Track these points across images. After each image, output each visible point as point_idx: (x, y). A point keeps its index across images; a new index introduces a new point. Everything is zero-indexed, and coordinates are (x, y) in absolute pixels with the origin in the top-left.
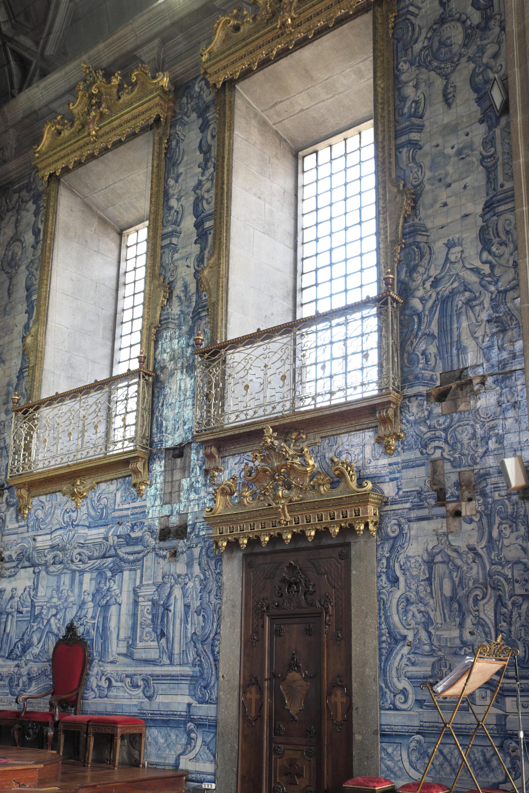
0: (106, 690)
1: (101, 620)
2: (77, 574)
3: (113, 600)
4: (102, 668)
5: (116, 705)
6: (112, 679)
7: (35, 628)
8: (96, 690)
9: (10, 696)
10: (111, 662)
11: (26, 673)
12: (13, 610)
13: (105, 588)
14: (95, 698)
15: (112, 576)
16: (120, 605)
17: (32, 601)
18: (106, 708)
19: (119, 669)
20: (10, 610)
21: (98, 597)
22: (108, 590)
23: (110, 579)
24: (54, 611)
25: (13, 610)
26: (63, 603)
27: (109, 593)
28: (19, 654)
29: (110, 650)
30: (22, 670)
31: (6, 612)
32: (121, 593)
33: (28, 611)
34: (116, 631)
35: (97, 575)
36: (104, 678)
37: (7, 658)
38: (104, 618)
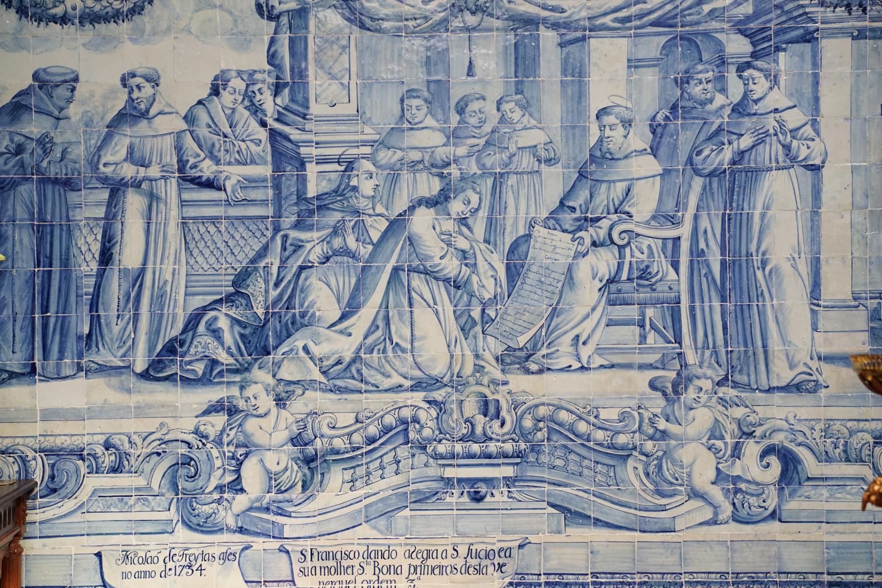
0: (773, 491)
1: (711, 224)
2: (548, 38)
3: (772, 150)
4: (739, 412)
5: (829, 546)
6: (803, 453)
7: (315, 253)
8: (716, 493)
9: (182, 534)
10: (786, 389)
11: (282, 436)
12: (154, 171)
13: (720, 100)
14: (714, 522)
15: (755, 55)
16: (815, 169)
17: (274, 134)
18: (779, 557)
19: (834, 413)
20: (129, 171)
21: (686, 139)
22: (740, 109)
23: (741, 69)
24: (430, 186)
25: (154, 171)
26: (477, 153)
27: (747, 122)
28: (223, 357)
29: (775, 344)
30: (251, 425)
31: (105, 180)
32: (814, 123)
33: (251, 182)
34: (804, 269)
35: (667, 48)
36: (752, 449)
37: (145, 376)
38: (726, 220)
